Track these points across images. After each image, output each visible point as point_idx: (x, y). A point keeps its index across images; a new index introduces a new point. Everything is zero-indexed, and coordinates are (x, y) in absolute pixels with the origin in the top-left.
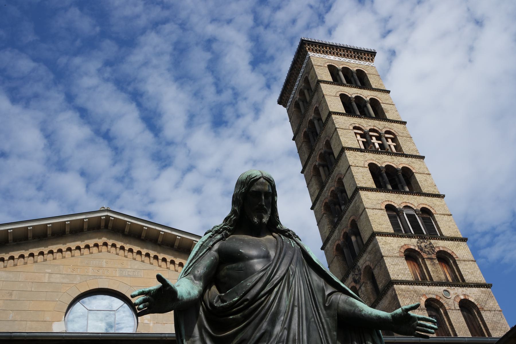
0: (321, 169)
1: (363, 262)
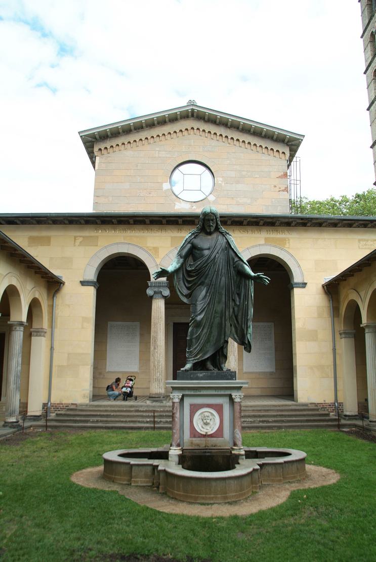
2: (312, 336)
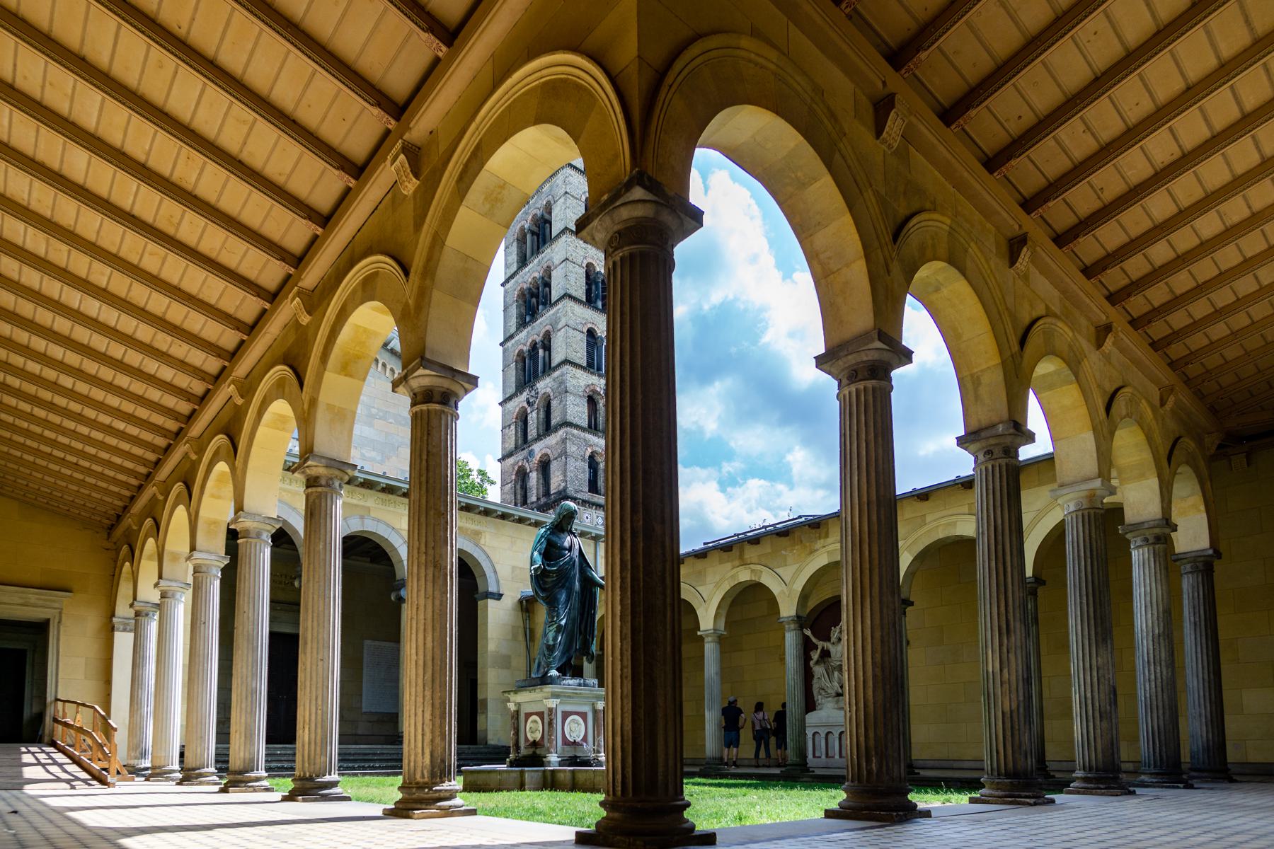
0: (529, 237)
1: (544, 385)
2: (505, 662)
